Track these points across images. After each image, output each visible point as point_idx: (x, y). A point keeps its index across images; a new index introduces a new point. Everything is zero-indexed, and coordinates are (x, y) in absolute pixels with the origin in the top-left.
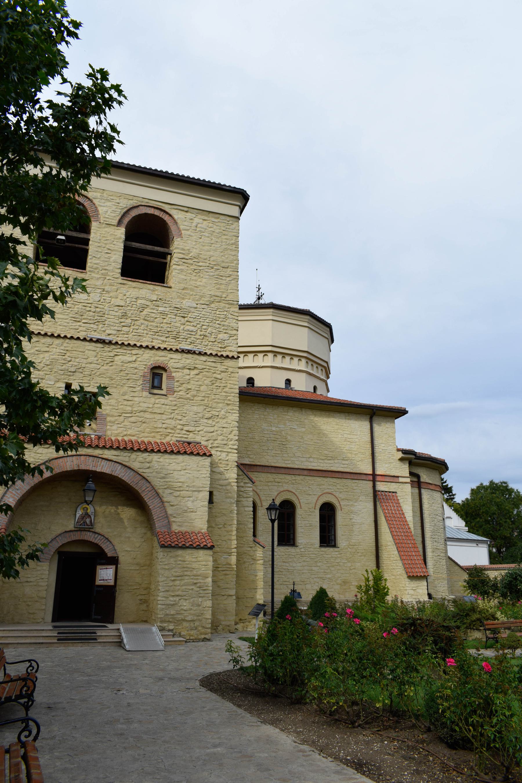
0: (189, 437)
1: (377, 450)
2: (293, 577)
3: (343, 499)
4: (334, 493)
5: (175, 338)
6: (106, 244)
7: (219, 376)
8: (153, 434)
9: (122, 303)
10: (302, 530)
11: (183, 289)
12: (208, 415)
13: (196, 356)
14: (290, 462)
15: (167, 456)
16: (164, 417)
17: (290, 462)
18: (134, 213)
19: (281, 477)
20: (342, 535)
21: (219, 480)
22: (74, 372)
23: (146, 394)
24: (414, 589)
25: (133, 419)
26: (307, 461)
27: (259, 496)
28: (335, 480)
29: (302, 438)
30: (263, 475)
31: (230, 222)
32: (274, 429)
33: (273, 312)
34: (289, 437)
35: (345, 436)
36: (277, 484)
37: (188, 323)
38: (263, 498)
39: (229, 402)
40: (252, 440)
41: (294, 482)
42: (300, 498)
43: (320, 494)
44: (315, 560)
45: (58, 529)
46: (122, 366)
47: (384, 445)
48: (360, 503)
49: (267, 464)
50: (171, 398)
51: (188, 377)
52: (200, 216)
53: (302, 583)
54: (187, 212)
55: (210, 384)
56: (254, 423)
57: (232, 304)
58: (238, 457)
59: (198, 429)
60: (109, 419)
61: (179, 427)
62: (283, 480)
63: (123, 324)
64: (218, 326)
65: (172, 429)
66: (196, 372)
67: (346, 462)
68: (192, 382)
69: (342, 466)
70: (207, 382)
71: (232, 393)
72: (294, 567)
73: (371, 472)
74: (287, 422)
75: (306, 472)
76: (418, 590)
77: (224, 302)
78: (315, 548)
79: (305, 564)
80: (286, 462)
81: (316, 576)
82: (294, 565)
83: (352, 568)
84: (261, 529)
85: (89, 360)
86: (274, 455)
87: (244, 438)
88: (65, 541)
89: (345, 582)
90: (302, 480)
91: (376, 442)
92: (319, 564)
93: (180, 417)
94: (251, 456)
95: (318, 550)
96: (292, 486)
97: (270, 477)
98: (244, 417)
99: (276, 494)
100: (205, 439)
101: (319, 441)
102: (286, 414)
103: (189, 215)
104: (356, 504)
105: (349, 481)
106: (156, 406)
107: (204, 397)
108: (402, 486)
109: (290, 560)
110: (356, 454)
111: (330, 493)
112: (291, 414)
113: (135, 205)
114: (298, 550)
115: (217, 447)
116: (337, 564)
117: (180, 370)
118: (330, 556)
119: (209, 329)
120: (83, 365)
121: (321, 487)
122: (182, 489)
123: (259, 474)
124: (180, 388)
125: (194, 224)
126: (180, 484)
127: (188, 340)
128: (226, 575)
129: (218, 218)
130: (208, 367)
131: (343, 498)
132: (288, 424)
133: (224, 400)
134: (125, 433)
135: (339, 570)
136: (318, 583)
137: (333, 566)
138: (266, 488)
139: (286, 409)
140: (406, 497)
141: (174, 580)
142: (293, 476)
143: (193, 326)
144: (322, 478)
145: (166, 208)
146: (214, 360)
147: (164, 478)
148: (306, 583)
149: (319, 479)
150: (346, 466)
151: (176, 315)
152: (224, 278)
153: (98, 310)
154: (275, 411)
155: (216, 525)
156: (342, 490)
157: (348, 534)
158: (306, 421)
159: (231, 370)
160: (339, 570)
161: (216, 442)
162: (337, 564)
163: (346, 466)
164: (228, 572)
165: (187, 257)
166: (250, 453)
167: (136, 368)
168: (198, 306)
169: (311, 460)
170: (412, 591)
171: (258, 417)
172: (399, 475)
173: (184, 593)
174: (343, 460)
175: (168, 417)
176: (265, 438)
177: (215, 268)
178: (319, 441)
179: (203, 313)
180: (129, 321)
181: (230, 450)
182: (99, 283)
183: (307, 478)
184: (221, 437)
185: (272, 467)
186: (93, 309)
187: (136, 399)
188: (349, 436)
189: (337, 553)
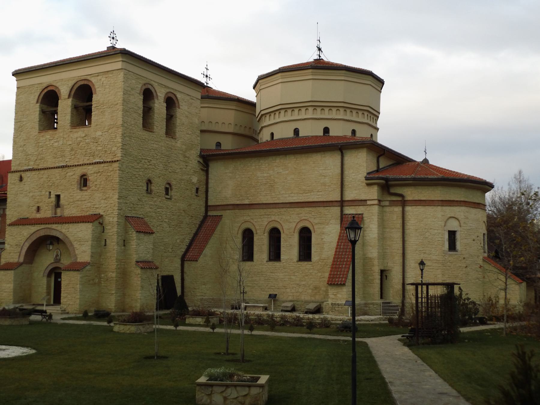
0: (97, 211)
1: (347, 179)
2: (277, 283)
3: (316, 224)
4: (310, 219)
5: (93, 156)
6: (64, 111)
7: (109, 174)
8: (82, 212)
9: (70, 143)
10: (285, 249)
11: (96, 126)
12: (104, 198)
13: (99, 165)
14: (276, 199)
15: (75, 225)
16: (86, 202)
17: (276, 199)
18: (75, 88)
19: (270, 211)
20: (315, 252)
21: (108, 233)
22: (51, 186)
23: (78, 191)
24: (335, 294)
25: (73, 206)
26: (289, 196)
27: (255, 226)
28: (310, 209)
29: (286, 179)
30: (257, 210)
31: (119, 73)
32: (265, 175)
33: (281, 76)
34: (276, 180)
35: (321, 172)
36: (267, 216)
37: (99, 146)
38: (257, 227)
39: (113, 189)
40: (250, 186)
41: (279, 213)
42: (283, 225)
43: (298, 221)
44: (293, 271)
45: (48, 262)
46: (69, 178)
47: (354, 174)
48: (330, 225)
49: (260, 202)
50: (89, 191)
51: (96, 178)
52: (104, 76)
53: (283, 288)
54: (98, 76)
55: (105, 179)
56: (251, 173)
57: (118, 127)
58: (118, 219)
59: (100, 206)
60: (65, 207)
61: (92, 206)
62: (271, 213)
63: (72, 154)
64: (112, 143)
65: (89, 208)
66: (99, 174)
67: (321, 193)
68: (98, 180)
69: (317, 197)
70: (104, 179)
71: (115, 182)
72: (278, 276)
73: (340, 200)
74: (275, 168)
75: (288, 205)
76: (338, 295)
77: (115, 127)
78: (294, 262)
79: (287, 274)
80: (274, 199)
81: (294, 283)
82: (278, 274)
83: (322, 277)
84: (256, 250)
85: (57, 178)
86: (265, 195)
87: (245, 185)
88: (54, 266)
89: (316, 288)
90: (285, 211)
91: (346, 173)
92: (297, 274)
93: (92, 201)
94: (250, 198)
95: (296, 263)
96: (277, 216)
97: (262, 211)
98: (245, 170)
99: (266, 224)
100: (103, 211)
101: (299, 179)
102: (274, 161)
103: (99, 78)
104: (327, 227)
105: (322, 208)
106: (82, 196)
107: (103, 187)
108: (369, 208)
109: (275, 271)
110: (329, 186)
111: (306, 220)
112: (278, 161)
113: (75, 82)
114: (281, 264)
115: (109, 215)
116: (310, 274)
117: (93, 175)
118: (304, 268)
119: (108, 146)
120: (55, 181)
121: (299, 216)
122: (80, 241)
123: (255, 210)
124: (93, 185)
125: (102, 83)
126: (79, 239)
127: (99, 156)
128: (111, 283)
129: (113, 73)
130: (105, 170)
131: (316, 222)
132: (276, 169)
133: (111, 188)
134: (71, 213)
135: (311, 278)
136: (295, 287)
137: (307, 276)
138: (259, 220)
139: (274, 157)
140: (373, 217)
141: (66, 286)
142: (278, 209)
143: (101, 146)
144: (299, 208)
145: (88, 78)
146: (107, 165)
147: (73, 236)
148: (286, 288)
149: (297, 210)
150: (320, 196)
151: (93, 142)
152: (115, 112)
153: (62, 149)
154: (267, 161)
155: (107, 257)
156: (315, 217)
157: (320, 250)
158: (289, 165)
159: (115, 169)
160: (311, 278)
161: (108, 212)
162: (310, 274)
163: (320, 196)
164: (112, 282)
165: (98, 105)
166: (248, 196)
167: (74, 178)
168: (103, 134)
169: (293, 195)
170: (333, 295)
171: (254, 168)
172: (367, 199)
173: (69, 292)
174: (318, 191)
175: (88, 201)
176: (259, 183)
177: (111, 107)
178: (299, 179)
179: (105, 137)
180: (74, 152)
181: (114, 216)
182: (61, 135)
183: (289, 209)
184: (110, 209)
185: (263, 204)
186: (60, 150)
187: (75, 195)
188: (324, 171)
189: (311, 266)
